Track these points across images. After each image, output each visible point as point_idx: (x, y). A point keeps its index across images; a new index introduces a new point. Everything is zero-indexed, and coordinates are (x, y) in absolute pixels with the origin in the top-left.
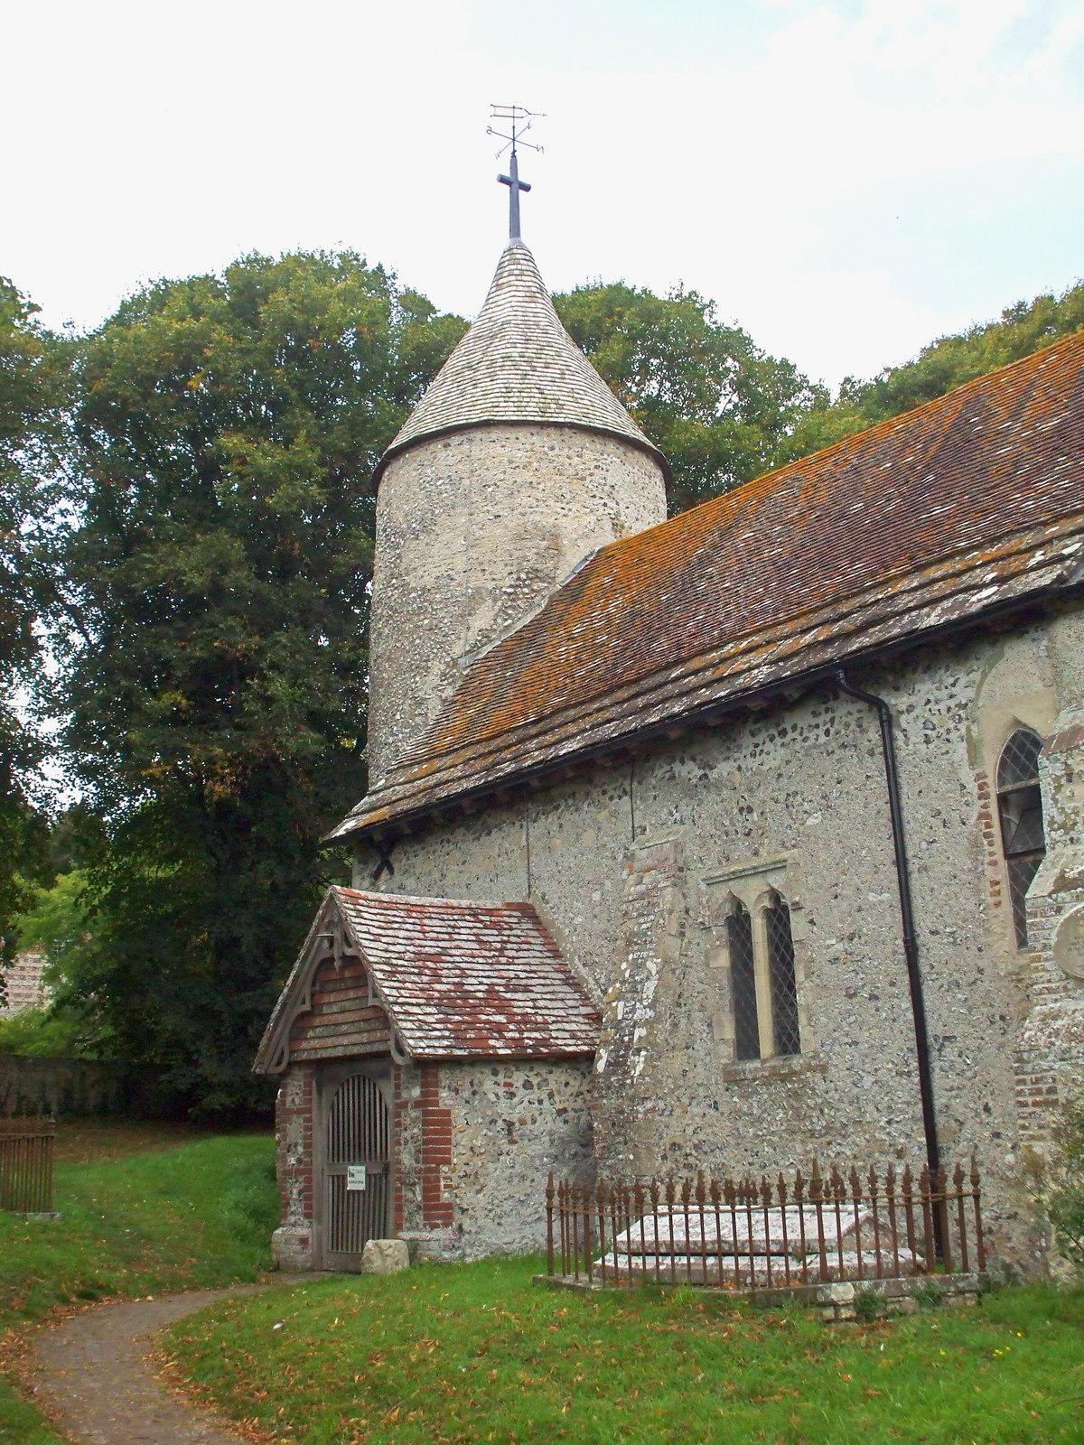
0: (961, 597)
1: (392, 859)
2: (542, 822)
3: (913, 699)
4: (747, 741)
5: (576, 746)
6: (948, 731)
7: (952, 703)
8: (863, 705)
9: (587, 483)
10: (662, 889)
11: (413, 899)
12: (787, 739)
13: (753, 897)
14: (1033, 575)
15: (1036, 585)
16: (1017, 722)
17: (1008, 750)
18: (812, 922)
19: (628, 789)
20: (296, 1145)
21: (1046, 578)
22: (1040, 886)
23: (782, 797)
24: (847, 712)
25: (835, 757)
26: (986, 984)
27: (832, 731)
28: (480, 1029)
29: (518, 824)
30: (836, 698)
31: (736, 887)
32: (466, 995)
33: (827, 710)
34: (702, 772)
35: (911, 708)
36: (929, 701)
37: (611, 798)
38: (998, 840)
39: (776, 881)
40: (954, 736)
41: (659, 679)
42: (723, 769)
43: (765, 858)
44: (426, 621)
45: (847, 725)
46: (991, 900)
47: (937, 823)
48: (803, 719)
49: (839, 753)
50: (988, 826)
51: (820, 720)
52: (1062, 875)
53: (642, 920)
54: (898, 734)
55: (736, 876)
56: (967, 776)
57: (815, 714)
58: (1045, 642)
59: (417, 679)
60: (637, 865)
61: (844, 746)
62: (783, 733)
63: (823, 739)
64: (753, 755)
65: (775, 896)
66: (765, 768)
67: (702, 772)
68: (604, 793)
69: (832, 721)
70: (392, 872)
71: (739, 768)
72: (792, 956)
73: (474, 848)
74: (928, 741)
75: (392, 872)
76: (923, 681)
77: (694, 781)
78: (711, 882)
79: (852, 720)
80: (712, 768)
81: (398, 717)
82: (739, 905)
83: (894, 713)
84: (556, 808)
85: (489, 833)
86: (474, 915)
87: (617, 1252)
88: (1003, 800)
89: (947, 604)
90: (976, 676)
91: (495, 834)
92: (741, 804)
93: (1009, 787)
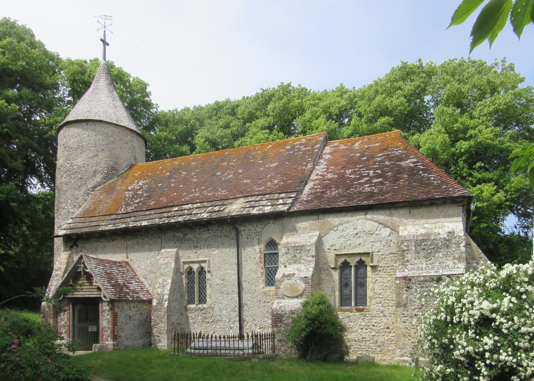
0: (261, 207)
1: (77, 243)
2: (131, 241)
3: (245, 229)
4: (198, 231)
5: (146, 224)
6: (253, 237)
7: (256, 231)
8: (232, 227)
9: (128, 145)
10: (171, 263)
11: (101, 258)
12: (209, 232)
13: (195, 267)
14: (280, 206)
15: (283, 209)
16: (271, 238)
17: (268, 244)
18: (212, 275)
19: (160, 236)
20: (64, 319)
21: (285, 208)
22: (278, 276)
23: (206, 245)
24: (226, 229)
25: (223, 238)
27: (222, 232)
28: (124, 293)
29: (123, 240)
30: (224, 224)
31: (191, 265)
32: (119, 284)
33: (221, 227)
34: (183, 236)
35: (244, 230)
36: (249, 230)
37: (155, 238)
38: (263, 263)
39: (203, 265)
40: (255, 238)
41: (168, 209)
42: (190, 236)
43: (200, 259)
44: (80, 176)
45: (226, 231)
46: (260, 276)
47: (248, 257)
48: (215, 228)
49: (224, 238)
50: (261, 260)
51: (219, 229)
52: (284, 274)
53: (165, 269)
54: (240, 236)
57: (218, 227)
58: (281, 222)
60: (163, 256)
61: (225, 236)
62: (208, 230)
63: (219, 233)
65: (202, 268)
66: (202, 237)
67: (183, 236)
68: (153, 236)
69: (223, 230)
70: (77, 246)
71: (195, 237)
72: (206, 282)
73: (108, 244)
74: (248, 238)
75: (77, 246)
76: (248, 225)
77: (181, 238)
78: (185, 263)
79: (228, 230)
80: (186, 235)
81: (69, 201)
82: (191, 269)
83: (239, 230)
84: (137, 238)
85: (113, 241)
86: (115, 263)
87: (191, 349)
88: (265, 254)
89: (258, 208)
90: (263, 226)
91: (115, 242)
92: (195, 245)
93: (266, 252)
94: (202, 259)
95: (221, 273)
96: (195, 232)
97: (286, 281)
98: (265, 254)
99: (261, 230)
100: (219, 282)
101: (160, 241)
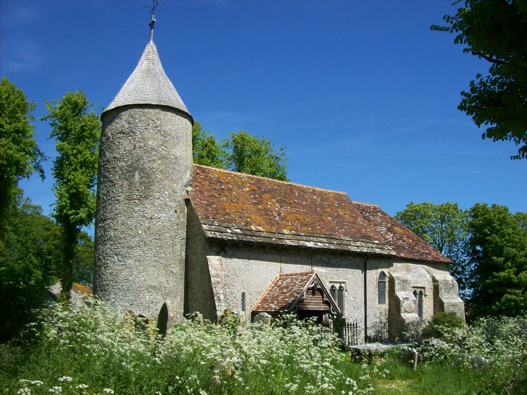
1: (226, 249)
13: (337, 286)
26: (374, 309)
31: (335, 284)
35: (369, 264)
37: (306, 258)
39: (343, 285)
43: (341, 280)
48: (351, 258)
55: (336, 282)
56: (375, 276)
59: (175, 184)
61: (357, 266)
64: (340, 261)
68: (304, 256)
71: (337, 262)
78: (330, 282)
88: (379, 282)
90: (379, 263)
91: (269, 255)
94: (343, 281)
95: (354, 292)
96: (337, 259)
97: (406, 302)
98: (379, 282)
99: (378, 265)
100: (352, 299)
101: (311, 261)
